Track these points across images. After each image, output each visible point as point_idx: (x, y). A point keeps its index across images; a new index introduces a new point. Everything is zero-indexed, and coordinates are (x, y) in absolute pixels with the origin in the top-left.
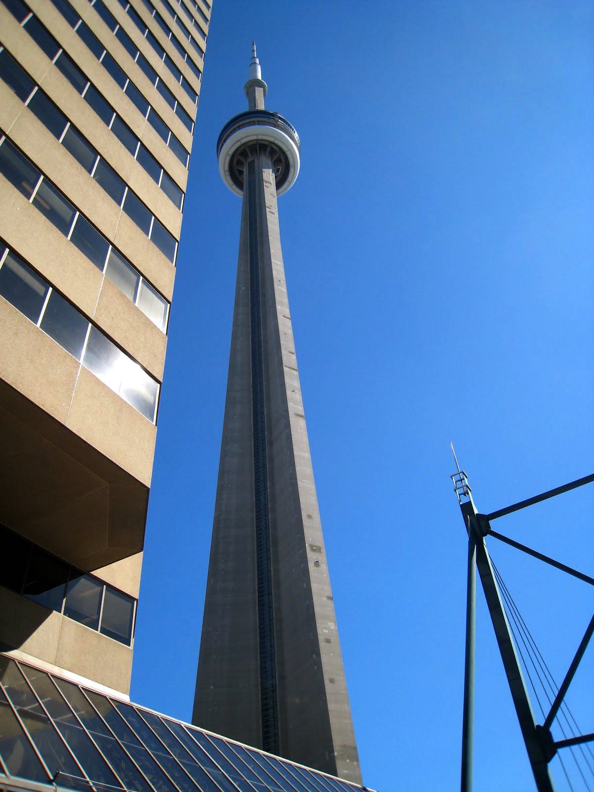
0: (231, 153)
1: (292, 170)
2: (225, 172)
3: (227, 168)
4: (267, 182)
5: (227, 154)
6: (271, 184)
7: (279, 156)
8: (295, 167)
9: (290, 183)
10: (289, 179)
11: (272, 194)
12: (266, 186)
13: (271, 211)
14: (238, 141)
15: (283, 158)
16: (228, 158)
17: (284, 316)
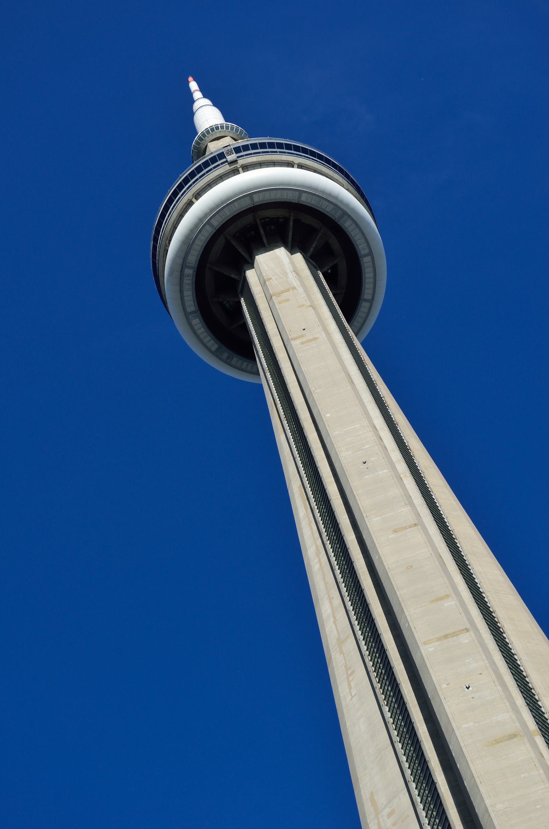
0: (191, 305)
1: (347, 225)
2: (217, 356)
3: (214, 345)
4: (279, 294)
5: (187, 315)
6: (294, 288)
7: (296, 221)
8: (346, 212)
9: (370, 253)
10: (362, 248)
11: (303, 306)
12: (280, 303)
13: (304, 339)
14: (182, 271)
15: (308, 220)
16: (197, 322)
17: (395, 531)
